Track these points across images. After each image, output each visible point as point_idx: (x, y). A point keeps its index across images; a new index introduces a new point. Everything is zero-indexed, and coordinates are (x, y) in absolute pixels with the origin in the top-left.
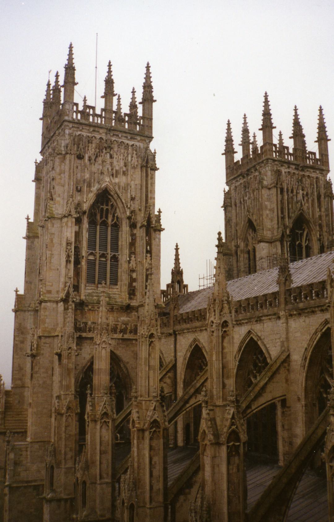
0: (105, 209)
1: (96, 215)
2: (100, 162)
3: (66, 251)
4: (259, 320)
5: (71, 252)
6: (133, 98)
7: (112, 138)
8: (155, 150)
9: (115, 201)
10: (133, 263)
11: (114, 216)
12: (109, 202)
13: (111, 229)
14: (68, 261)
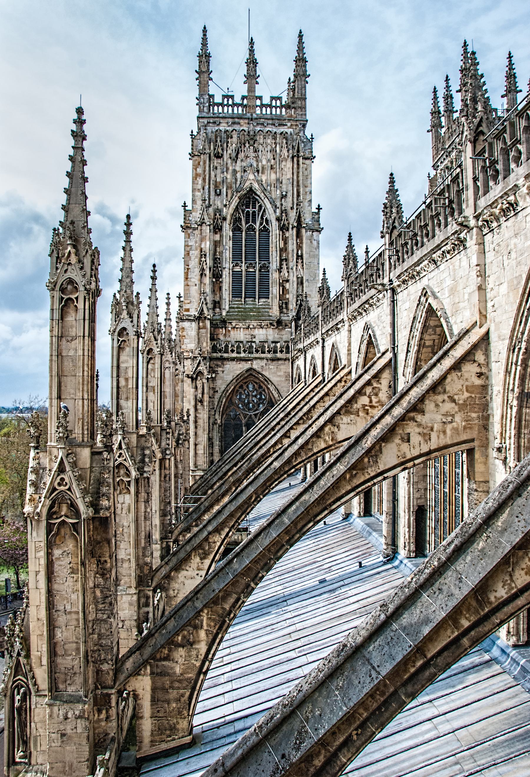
0: (251, 212)
10: (285, 271)
11: (262, 218)
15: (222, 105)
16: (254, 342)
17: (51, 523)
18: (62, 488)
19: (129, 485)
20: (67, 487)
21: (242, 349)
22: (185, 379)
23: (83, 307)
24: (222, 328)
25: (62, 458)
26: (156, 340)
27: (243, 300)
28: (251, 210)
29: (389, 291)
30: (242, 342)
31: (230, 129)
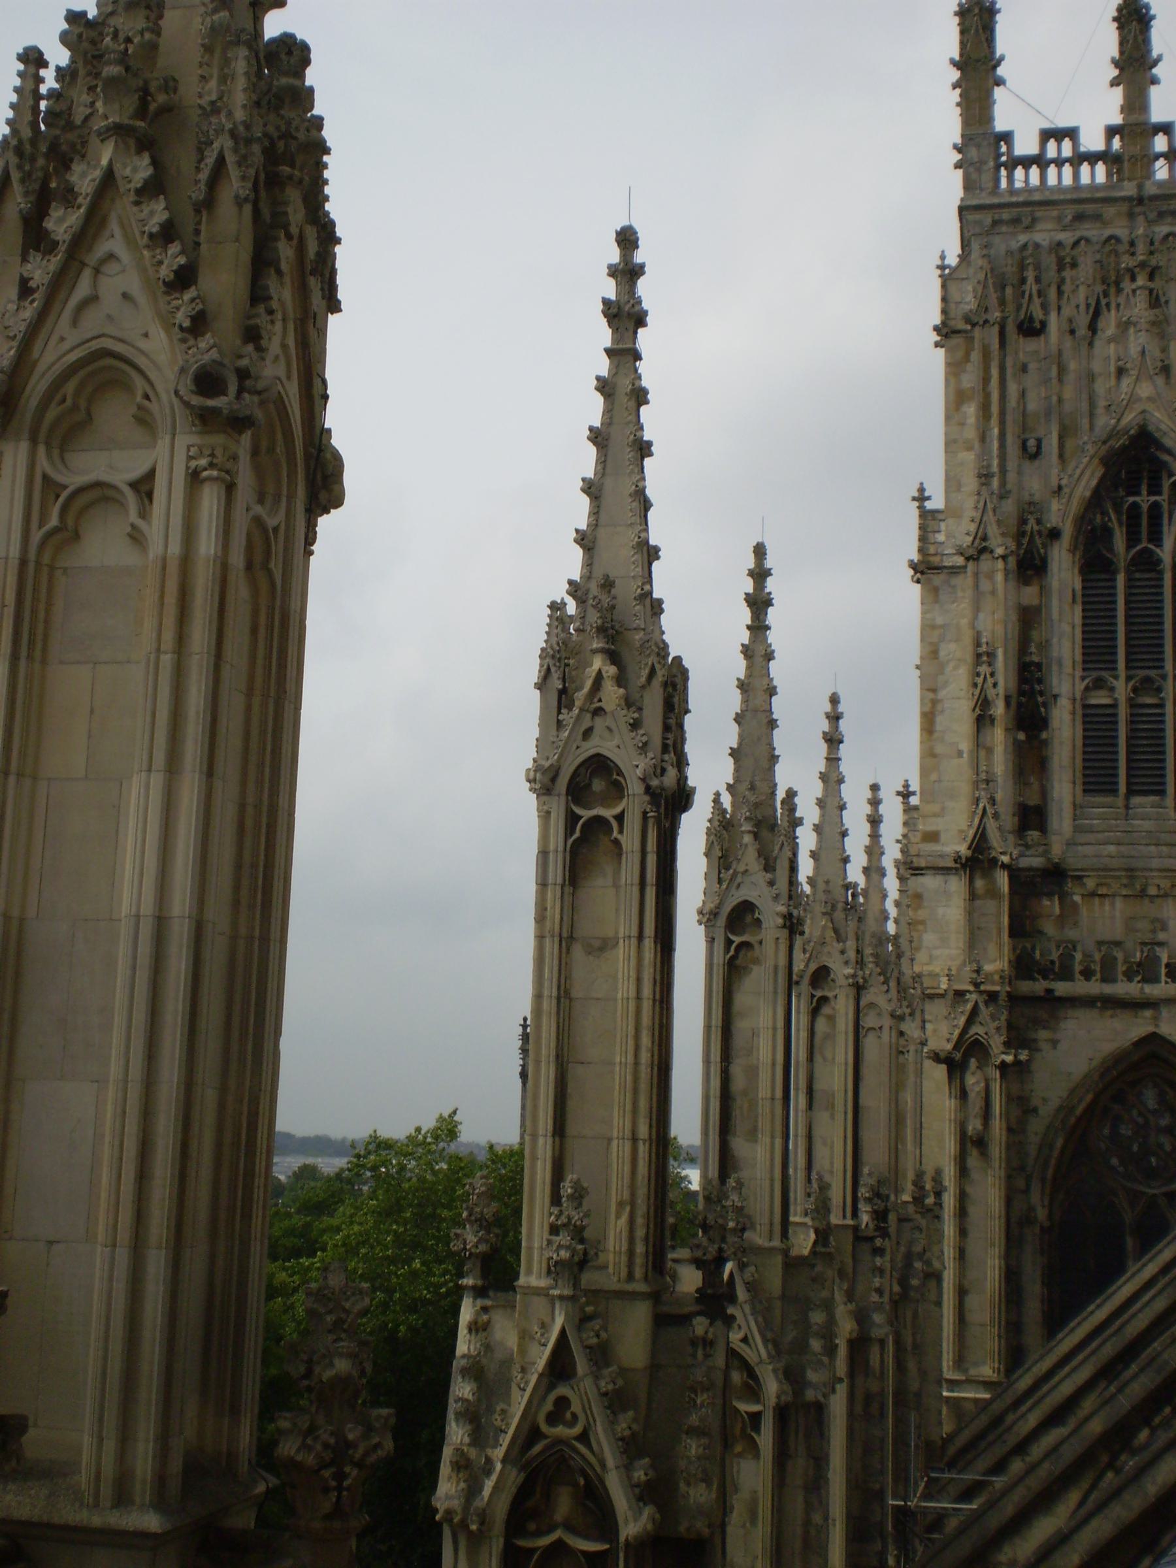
0: (1145, 507)
2: (1111, 331)
3: (975, 685)
5: (995, 685)
7: (1157, 229)
12: (1164, 475)
13: (1129, 579)
14: (983, 720)
15: (1040, 161)
16: (1161, 944)
17: (520, 1548)
18: (560, 1431)
20: (577, 1430)
21: (1121, 968)
22: (928, 1064)
23: (637, 845)
24: (1050, 895)
25: (563, 1332)
26: (839, 937)
27: (1120, 801)
28: (1144, 500)
30: (1118, 944)
31: (1067, 237)
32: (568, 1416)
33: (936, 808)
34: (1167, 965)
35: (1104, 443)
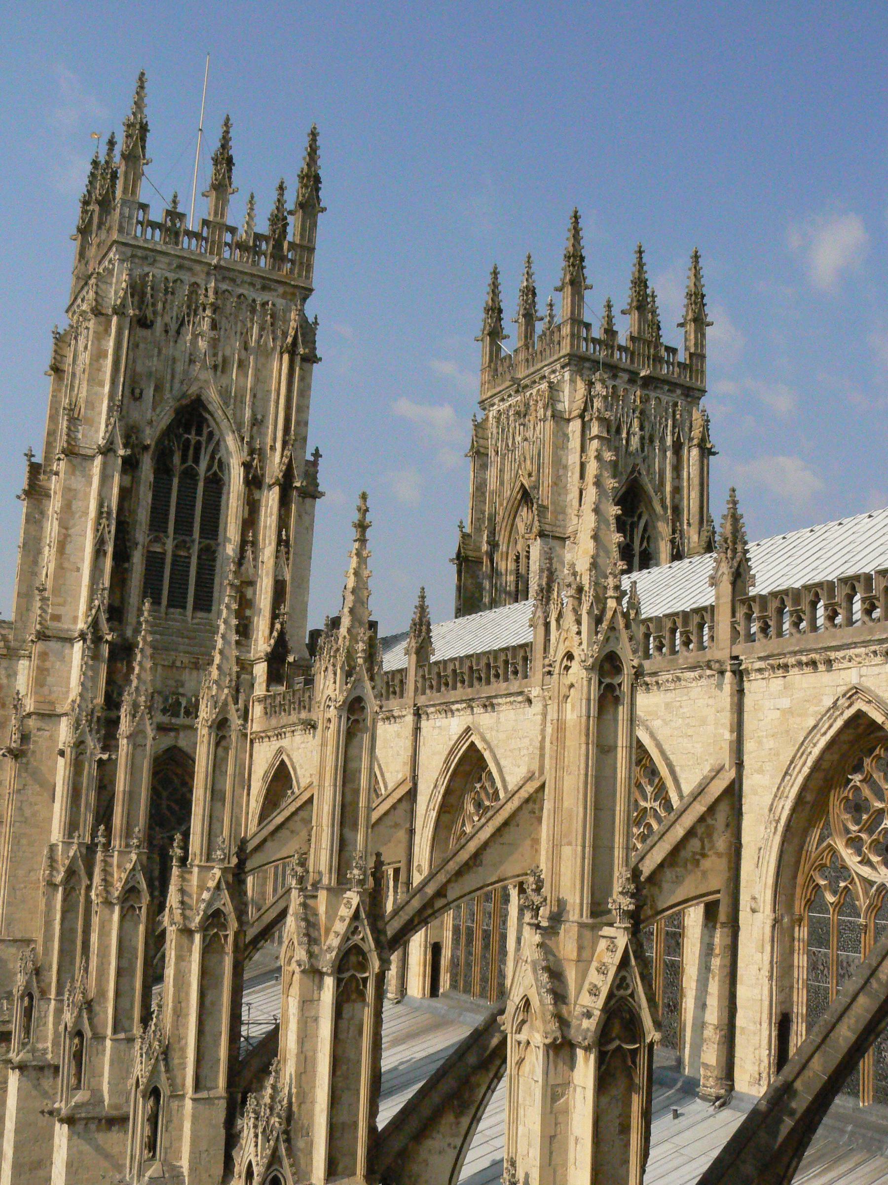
0: (193, 442)
1: (172, 453)
3: (98, 530)
4: (489, 705)
5: (109, 532)
6: (280, 202)
8: (316, 318)
9: (217, 424)
11: (212, 458)
14: (99, 552)
16: (183, 695)
18: (622, 992)
19: (365, 986)
20: (629, 991)
24: (122, 660)
28: (193, 437)
29: (728, 675)
31: (171, 276)
32: (624, 985)
33: (60, 600)
34: (185, 707)
35: (179, 400)
